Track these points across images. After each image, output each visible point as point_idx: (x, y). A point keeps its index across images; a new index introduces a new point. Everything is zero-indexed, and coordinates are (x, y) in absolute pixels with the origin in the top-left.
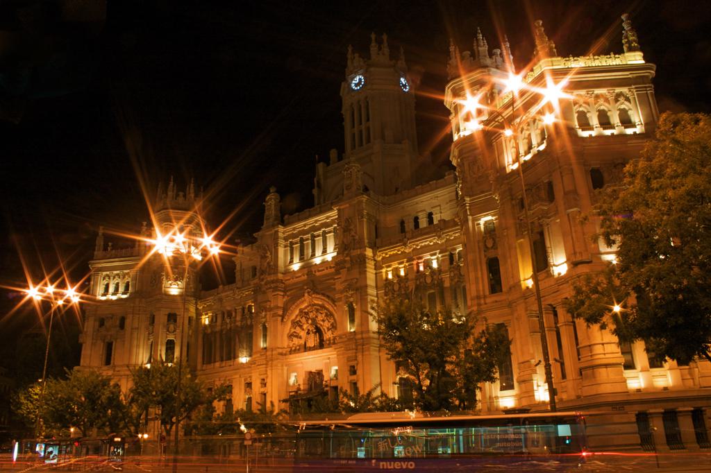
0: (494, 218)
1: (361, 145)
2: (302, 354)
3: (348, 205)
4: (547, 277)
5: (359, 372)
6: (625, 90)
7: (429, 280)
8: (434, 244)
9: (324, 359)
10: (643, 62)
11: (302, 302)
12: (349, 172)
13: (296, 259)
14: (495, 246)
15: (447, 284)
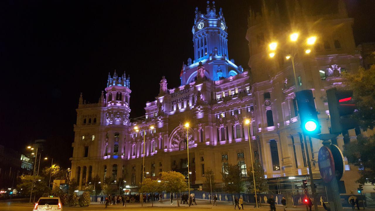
8: (239, 103)
12: (199, 70)
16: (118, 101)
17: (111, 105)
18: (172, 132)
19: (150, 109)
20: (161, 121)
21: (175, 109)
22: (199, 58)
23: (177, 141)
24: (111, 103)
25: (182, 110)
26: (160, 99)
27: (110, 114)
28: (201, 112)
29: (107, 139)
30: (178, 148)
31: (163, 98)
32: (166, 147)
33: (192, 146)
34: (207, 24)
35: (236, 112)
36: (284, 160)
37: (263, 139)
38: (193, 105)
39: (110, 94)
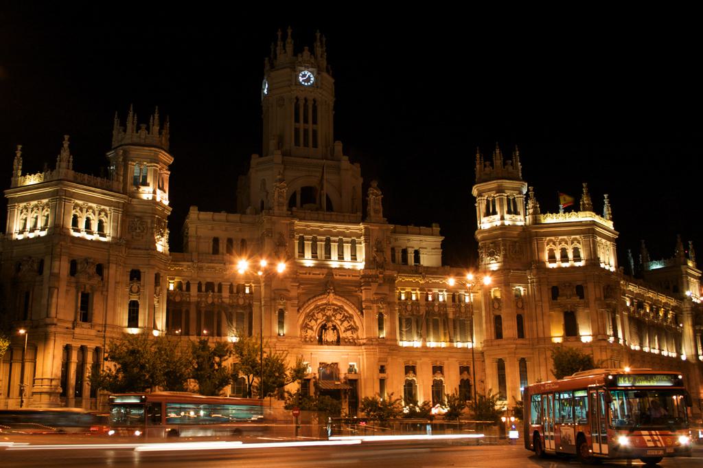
0: (522, 289)
1: (306, 145)
2: (315, 346)
3: (377, 228)
4: (575, 341)
5: (388, 371)
6: (608, 243)
7: (436, 309)
9: (343, 355)
10: (613, 228)
13: (308, 254)
14: (523, 308)
15: (451, 316)
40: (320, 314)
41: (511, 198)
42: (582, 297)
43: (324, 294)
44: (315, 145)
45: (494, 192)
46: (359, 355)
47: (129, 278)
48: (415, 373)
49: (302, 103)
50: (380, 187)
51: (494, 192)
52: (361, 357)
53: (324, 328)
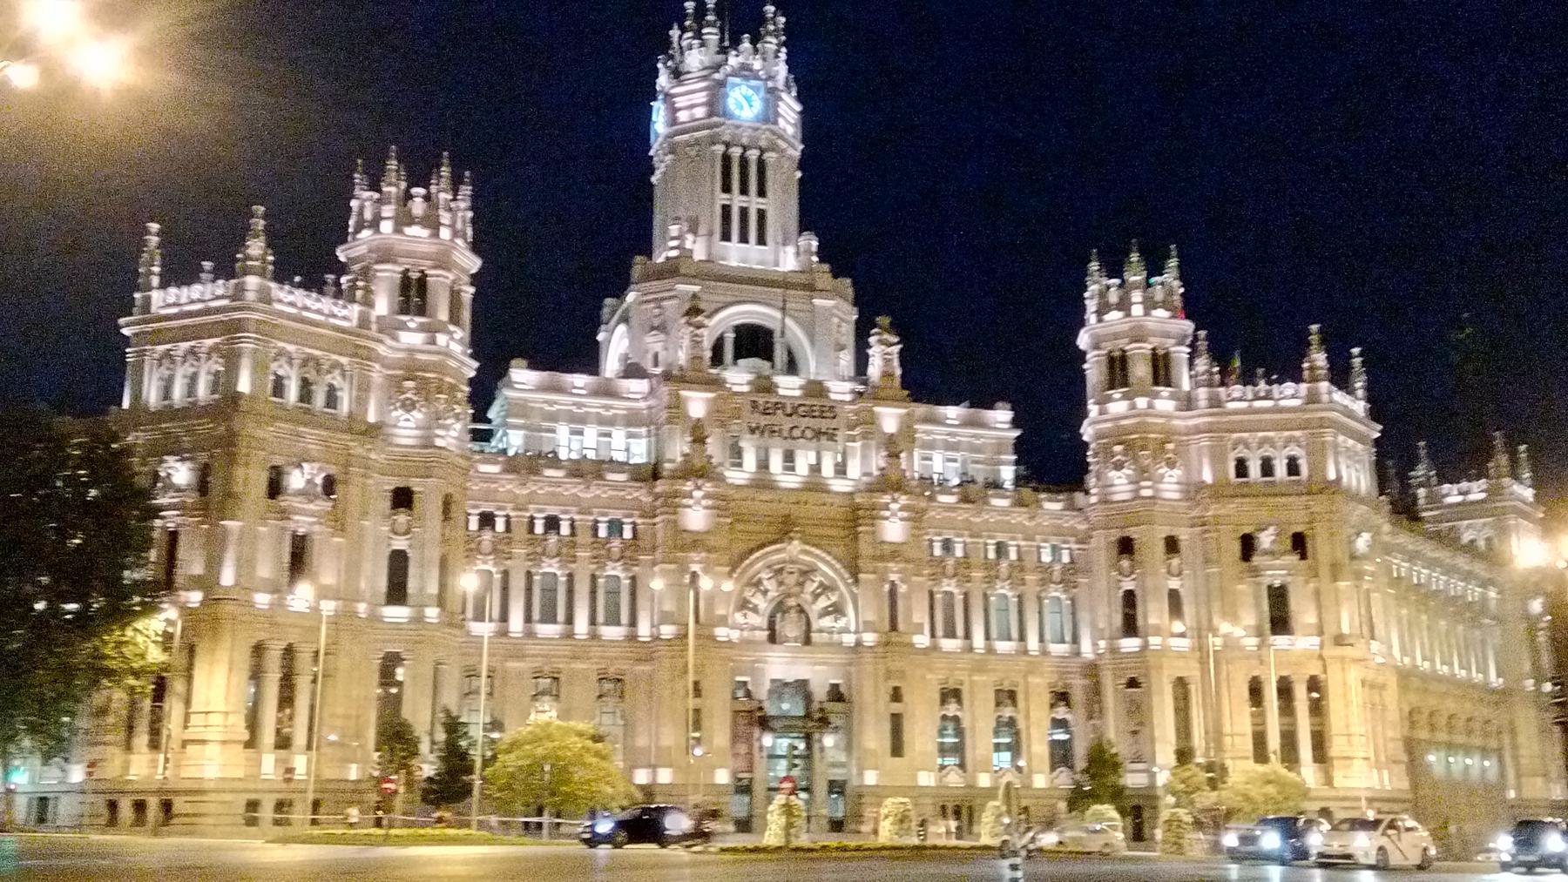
5: (906, 698)
11: (778, 551)
16: (452, 328)
17: (433, 342)
18: (747, 562)
19: (537, 405)
20: (704, 502)
21: (750, 461)
22: (726, 237)
23: (759, 601)
24: (431, 330)
25: (789, 481)
26: (687, 398)
27: (424, 388)
28: (902, 519)
29: (402, 518)
30: (767, 633)
31: (708, 400)
32: (723, 621)
33: (836, 636)
34: (770, 116)
35: (1001, 549)
36: (1228, 740)
37: (1166, 672)
38: (841, 470)
39: (415, 275)
40: (773, 581)
41: (1161, 352)
42: (1303, 557)
43: (782, 542)
44: (761, 240)
45: (1126, 340)
46: (850, 664)
47: (388, 504)
48: (959, 701)
49: (736, 152)
50: (895, 328)
51: (1126, 340)
52: (853, 669)
53: (780, 608)
